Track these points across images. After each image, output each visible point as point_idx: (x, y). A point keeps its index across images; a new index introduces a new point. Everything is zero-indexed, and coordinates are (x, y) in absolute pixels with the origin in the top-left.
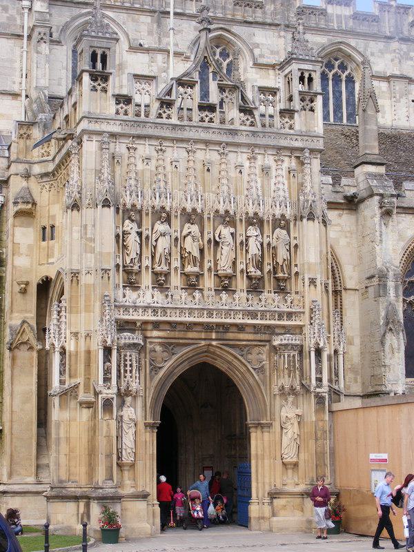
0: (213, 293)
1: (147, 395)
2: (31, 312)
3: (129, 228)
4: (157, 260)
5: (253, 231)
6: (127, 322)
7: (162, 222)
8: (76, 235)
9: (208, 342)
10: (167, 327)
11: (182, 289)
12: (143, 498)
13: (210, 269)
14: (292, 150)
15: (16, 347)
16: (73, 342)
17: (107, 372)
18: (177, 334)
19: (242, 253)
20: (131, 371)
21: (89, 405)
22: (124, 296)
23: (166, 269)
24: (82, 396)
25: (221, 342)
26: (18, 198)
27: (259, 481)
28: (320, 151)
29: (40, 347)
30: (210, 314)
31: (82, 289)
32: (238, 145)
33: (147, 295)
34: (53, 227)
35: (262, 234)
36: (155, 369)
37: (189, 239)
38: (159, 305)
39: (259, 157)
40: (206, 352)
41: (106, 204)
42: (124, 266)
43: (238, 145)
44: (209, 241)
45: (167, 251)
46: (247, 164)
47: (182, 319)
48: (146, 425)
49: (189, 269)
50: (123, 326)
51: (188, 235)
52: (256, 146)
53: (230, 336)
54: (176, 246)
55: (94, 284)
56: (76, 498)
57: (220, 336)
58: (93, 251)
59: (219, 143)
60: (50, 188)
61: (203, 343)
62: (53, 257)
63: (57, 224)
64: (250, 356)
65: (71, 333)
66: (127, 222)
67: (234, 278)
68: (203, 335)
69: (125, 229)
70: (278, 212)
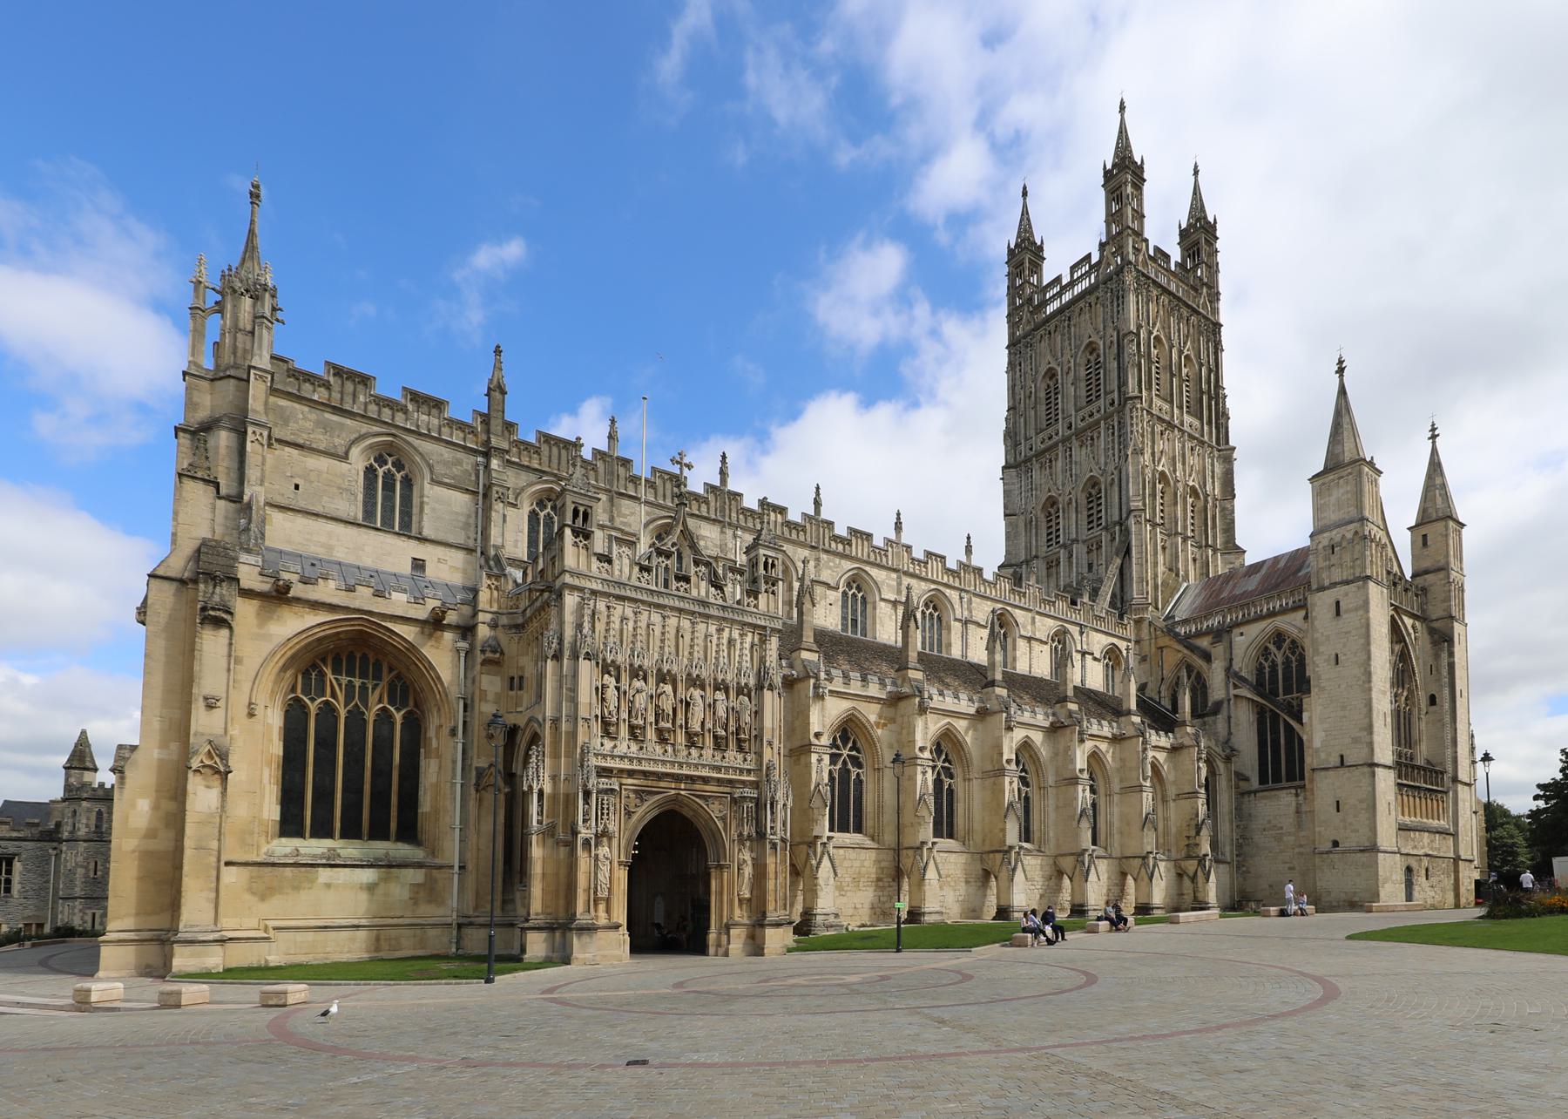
5: (720, 696)
6: (605, 769)
14: (755, 626)
17: (586, 813)
18: (650, 783)
20: (608, 814)
22: (602, 745)
23: (641, 722)
28: (779, 631)
32: (708, 617)
33: (625, 746)
34: (521, 678)
35: (727, 698)
39: (727, 630)
43: (708, 617)
44: (681, 701)
46: (715, 637)
47: (655, 769)
49: (662, 724)
50: (604, 772)
52: (724, 619)
59: (693, 613)
63: (527, 675)
70: (743, 681)
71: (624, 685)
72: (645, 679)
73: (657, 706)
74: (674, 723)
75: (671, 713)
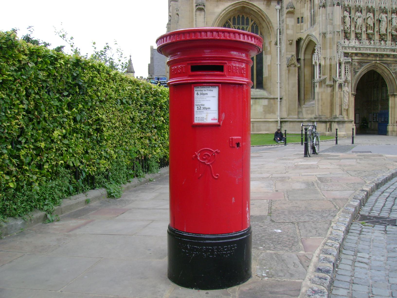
0: (378, 41)
1: (353, 82)
2: (294, 52)
3: (346, 15)
4: (357, 28)
7: (359, 12)
8: (324, 18)
9: (375, 62)
10: (360, 55)
11: (366, 40)
12: (351, 122)
13: (377, 32)
15: (290, 66)
16: (323, 61)
17: (340, 72)
18: (364, 58)
19: (389, 25)
20: (348, 73)
21: (331, 86)
22: (344, 42)
24: (328, 82)
25: (381, 62)
26: (288, 6)
27: (392, 116)
29: (299, 65)
30: (377, 50)
31: (328, 41)
33: (354, 42)
34: (302, 18)
36: (355, 72)
37: (369, 19)
38: (358, 46)
40: (373, 66)
41: (338, 4)
42: (344, 30)
44: (377, 20)
45: (361, 24)
48: (352, 94)
49: (370, 31)
50: (346, 55)
51: (369, 17)
53: (384, 59)
54: (364, 22)
55: (333, 38)
56: (325, 122)
57: (381, 59)
58: (332, 24)
60: (301, 2)
61: (374, 62)
62: (303, 30)
64: (391, 67)
65: (323, 58)
66: (345, 12)
67: (386, 35)
68: (374, 59)
69: (344, 15)
71: (352, 15)
72: (361, 12)
73: (367, 23)
74: (374, 31)
75: (372, 25)
